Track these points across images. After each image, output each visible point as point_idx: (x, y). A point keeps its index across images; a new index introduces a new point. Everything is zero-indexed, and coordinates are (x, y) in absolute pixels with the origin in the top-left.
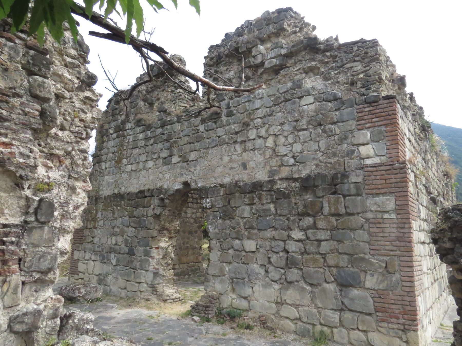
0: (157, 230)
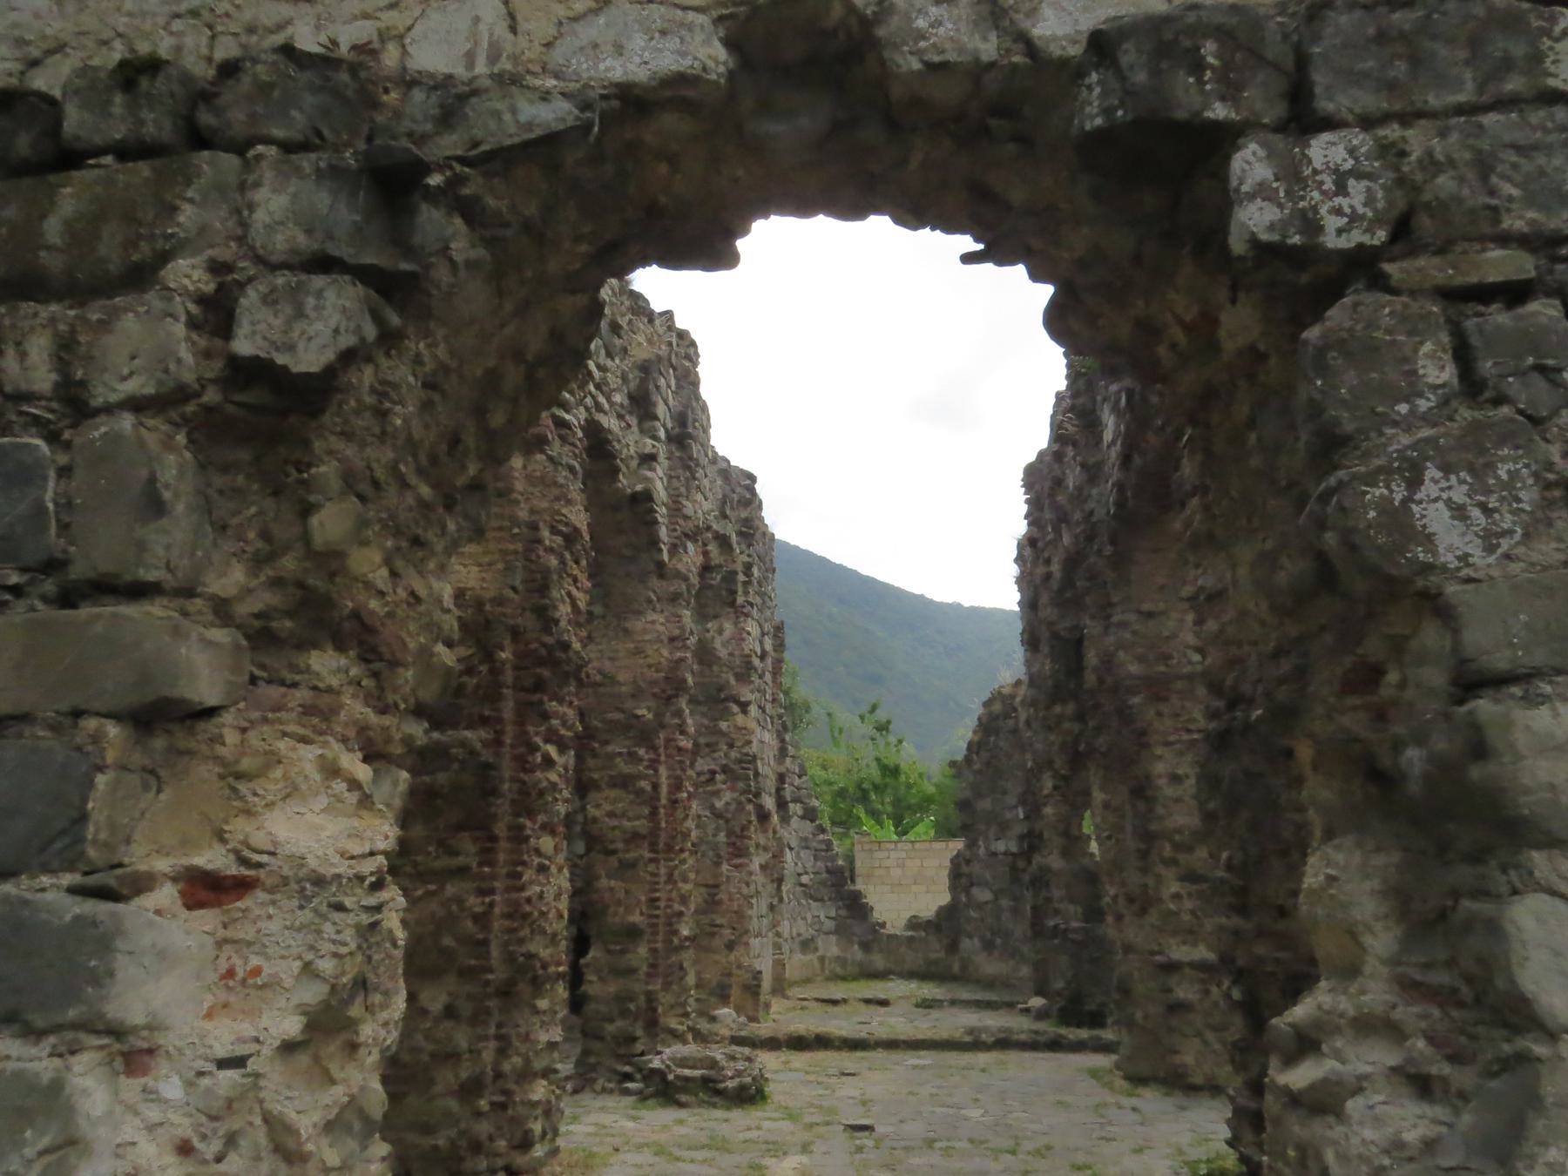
0: (222, 610)
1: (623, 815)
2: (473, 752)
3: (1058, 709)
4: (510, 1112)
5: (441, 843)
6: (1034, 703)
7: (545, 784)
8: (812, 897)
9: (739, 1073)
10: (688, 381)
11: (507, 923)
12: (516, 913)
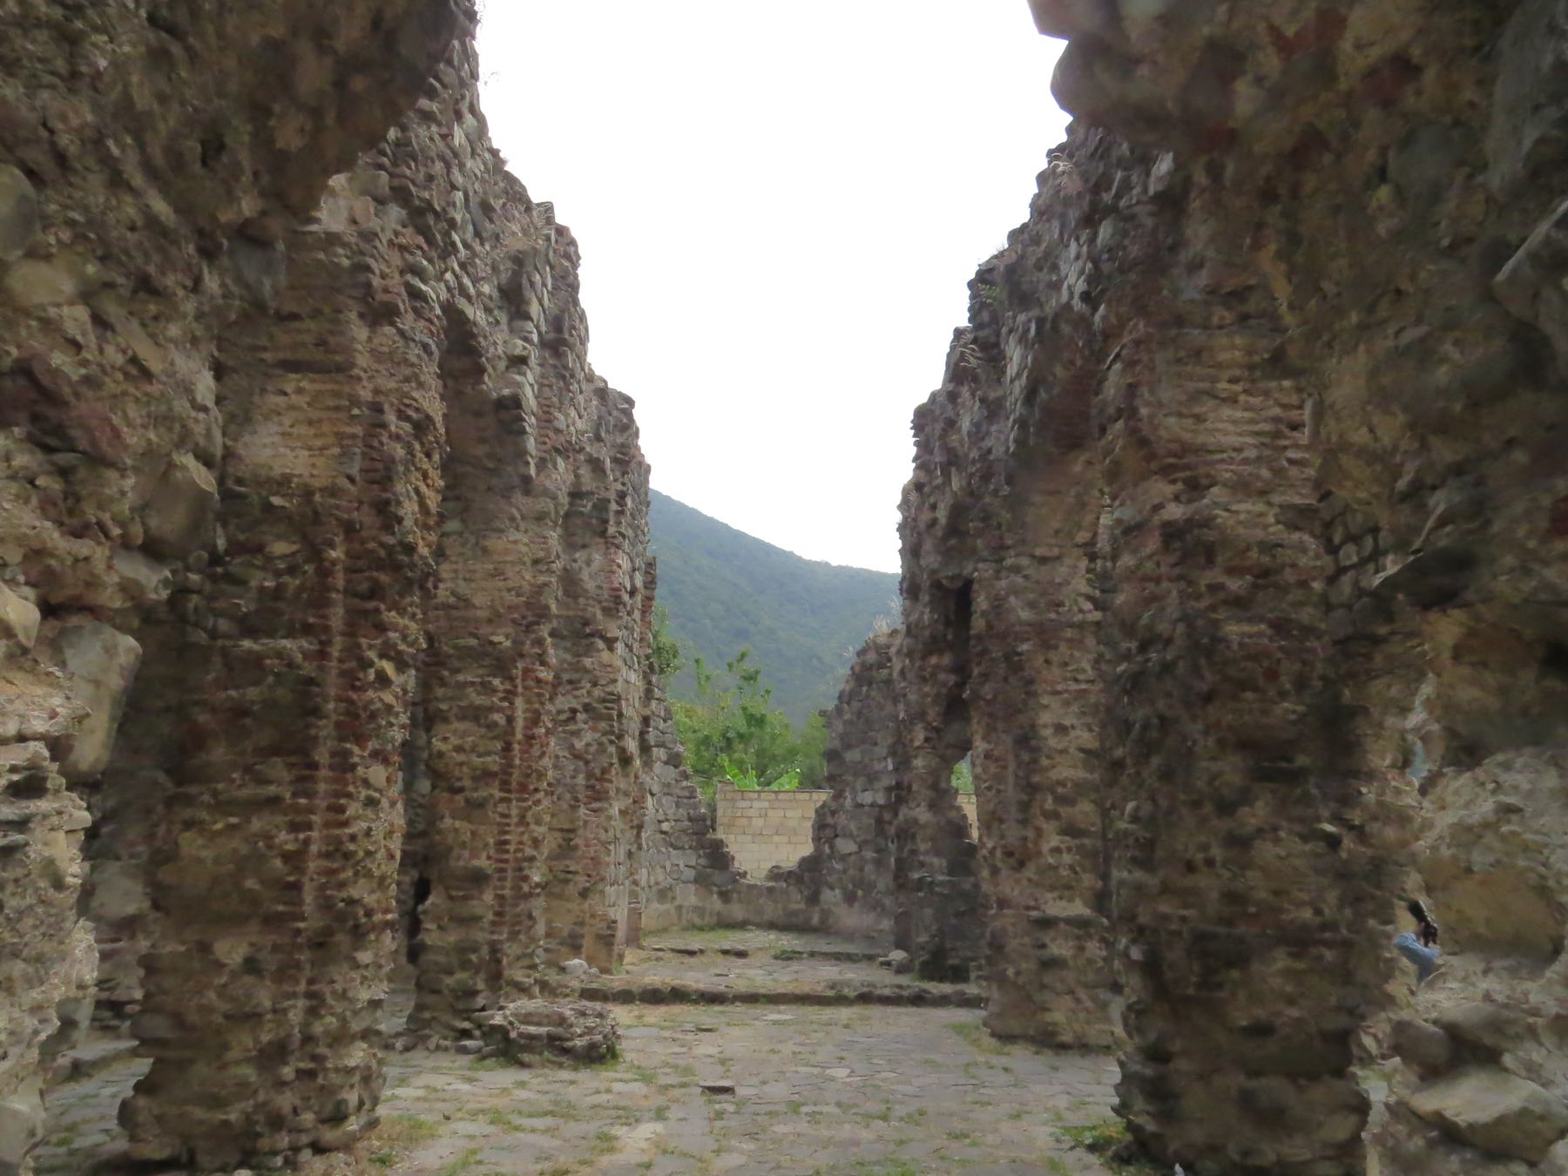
1: (473, 750)
2: (291, 665)
3: (934, 660)
4: (320, 1080)
5: (247, 769)
6: (910, 654)
7: (378, 705)
8: (671, 845)
9: (590, 1031)
10: (567, 285)
11: (325, 863)
12: (337, 852)
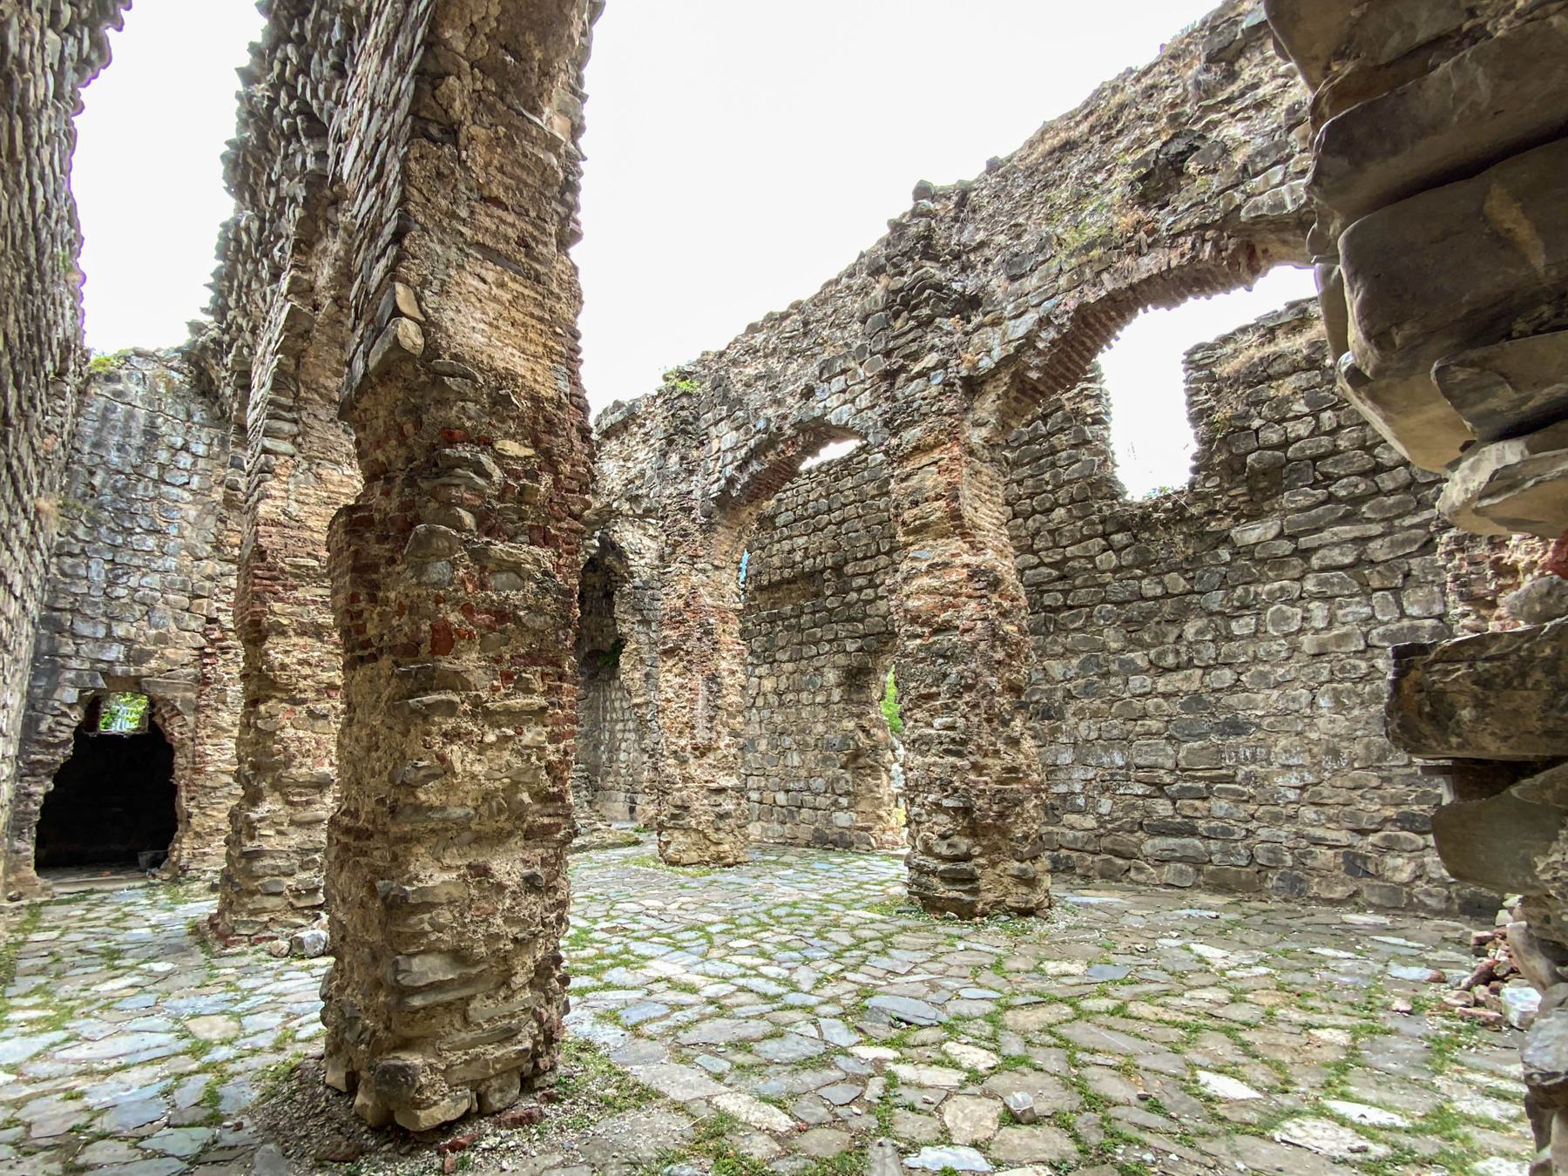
5: (507, 677)
